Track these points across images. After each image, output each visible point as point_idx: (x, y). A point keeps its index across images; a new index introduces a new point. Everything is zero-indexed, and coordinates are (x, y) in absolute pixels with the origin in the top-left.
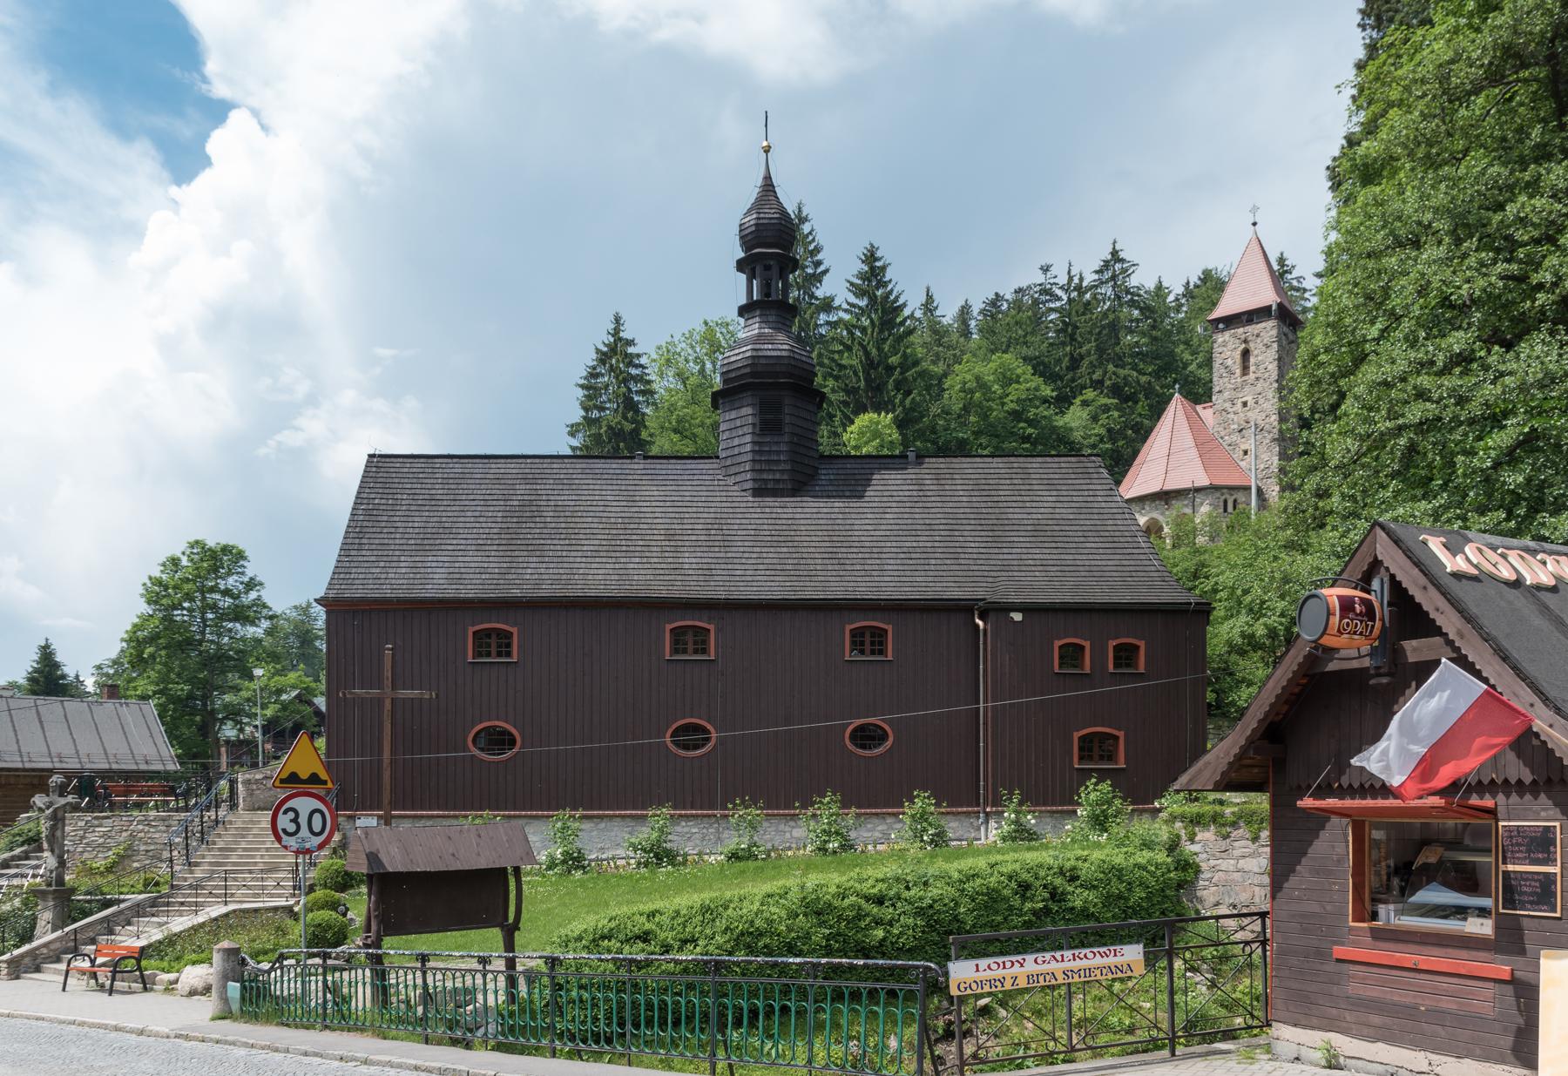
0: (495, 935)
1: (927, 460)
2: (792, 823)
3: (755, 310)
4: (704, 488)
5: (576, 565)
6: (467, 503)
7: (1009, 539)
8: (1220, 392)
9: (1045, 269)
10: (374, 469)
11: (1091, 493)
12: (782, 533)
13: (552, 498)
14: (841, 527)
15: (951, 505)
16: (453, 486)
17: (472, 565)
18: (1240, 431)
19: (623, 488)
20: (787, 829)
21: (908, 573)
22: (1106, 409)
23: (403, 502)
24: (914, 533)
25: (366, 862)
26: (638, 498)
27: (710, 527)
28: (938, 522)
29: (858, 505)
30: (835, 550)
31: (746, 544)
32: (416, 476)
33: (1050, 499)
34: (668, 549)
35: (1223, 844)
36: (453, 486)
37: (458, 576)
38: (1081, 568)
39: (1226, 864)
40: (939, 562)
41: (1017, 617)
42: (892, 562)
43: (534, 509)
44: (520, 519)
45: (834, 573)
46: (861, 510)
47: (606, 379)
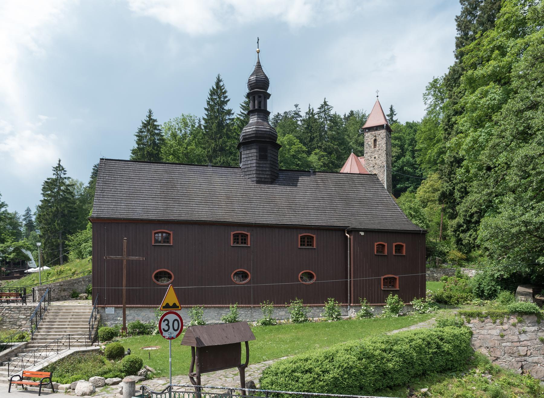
0: (236, 370)
1: (317, 173)
2: (279, 310)
4: (237, 179)
5: (194, 208)
6: (145, 180)
7: (352, 204)
8: (367, 153)
9: (296, 106)
10: (103, 165)
11: (377, 189)
12: (270, 198)
13: (179, 180)
14: (291, 197)
15: (329, 190)
16: (138, 173)
17: (152, 206)
19: (206, 178)
20: (277, 312)
21: (319, 216)
22: (323, 156)
23: (118, 179)
24: (318, 200)
25: (196, 342)
26: (212, 182)
27: (242, 194)
28: (326, 196)
29: (296, 189)
30: (291, 206)
31: (257, 202)
32: (121, 168)
33: (363, 190)
34: (228, 203)
35: (482, 324)
36: (138, 173)
37: (147, 210)
38: (379, 216)
39: (483, 332)
40: (329, 212)
41: (362, 234)
42: (312, 211)
43: (172, 184)
44: (168, 188)
45: (292, 215)
46: (297, 191)
47: (146, 133)
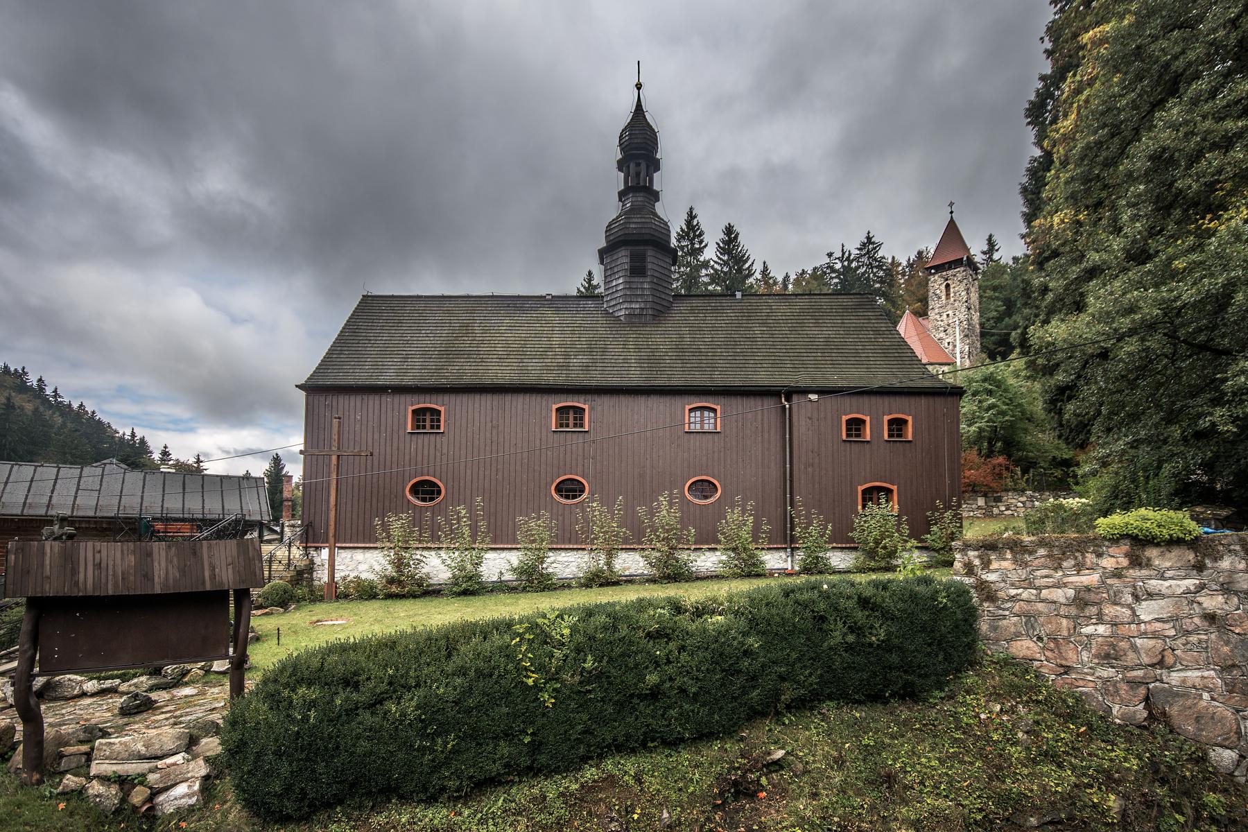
3: (629, 194)
8: (933, 309)
18: (945, 331)
41: (814, 397)
